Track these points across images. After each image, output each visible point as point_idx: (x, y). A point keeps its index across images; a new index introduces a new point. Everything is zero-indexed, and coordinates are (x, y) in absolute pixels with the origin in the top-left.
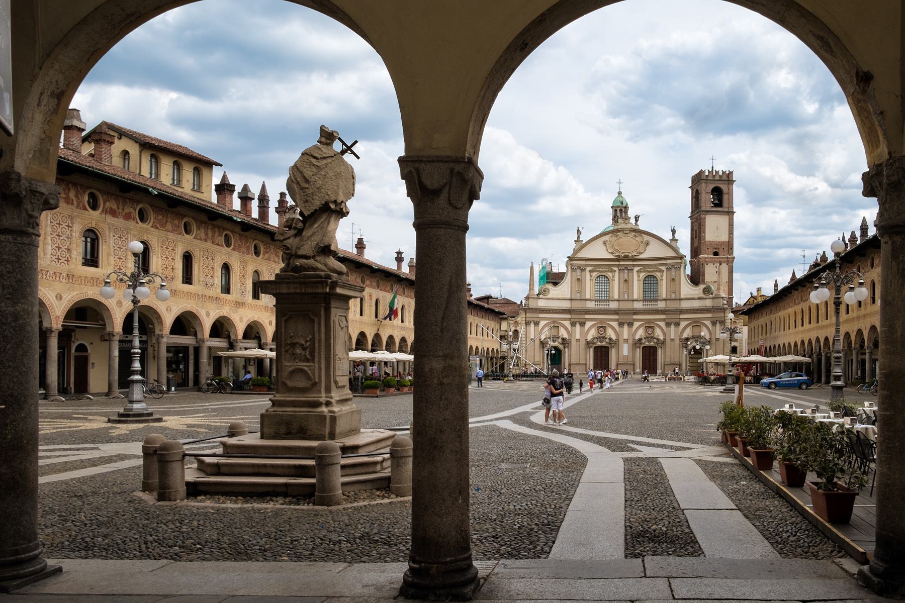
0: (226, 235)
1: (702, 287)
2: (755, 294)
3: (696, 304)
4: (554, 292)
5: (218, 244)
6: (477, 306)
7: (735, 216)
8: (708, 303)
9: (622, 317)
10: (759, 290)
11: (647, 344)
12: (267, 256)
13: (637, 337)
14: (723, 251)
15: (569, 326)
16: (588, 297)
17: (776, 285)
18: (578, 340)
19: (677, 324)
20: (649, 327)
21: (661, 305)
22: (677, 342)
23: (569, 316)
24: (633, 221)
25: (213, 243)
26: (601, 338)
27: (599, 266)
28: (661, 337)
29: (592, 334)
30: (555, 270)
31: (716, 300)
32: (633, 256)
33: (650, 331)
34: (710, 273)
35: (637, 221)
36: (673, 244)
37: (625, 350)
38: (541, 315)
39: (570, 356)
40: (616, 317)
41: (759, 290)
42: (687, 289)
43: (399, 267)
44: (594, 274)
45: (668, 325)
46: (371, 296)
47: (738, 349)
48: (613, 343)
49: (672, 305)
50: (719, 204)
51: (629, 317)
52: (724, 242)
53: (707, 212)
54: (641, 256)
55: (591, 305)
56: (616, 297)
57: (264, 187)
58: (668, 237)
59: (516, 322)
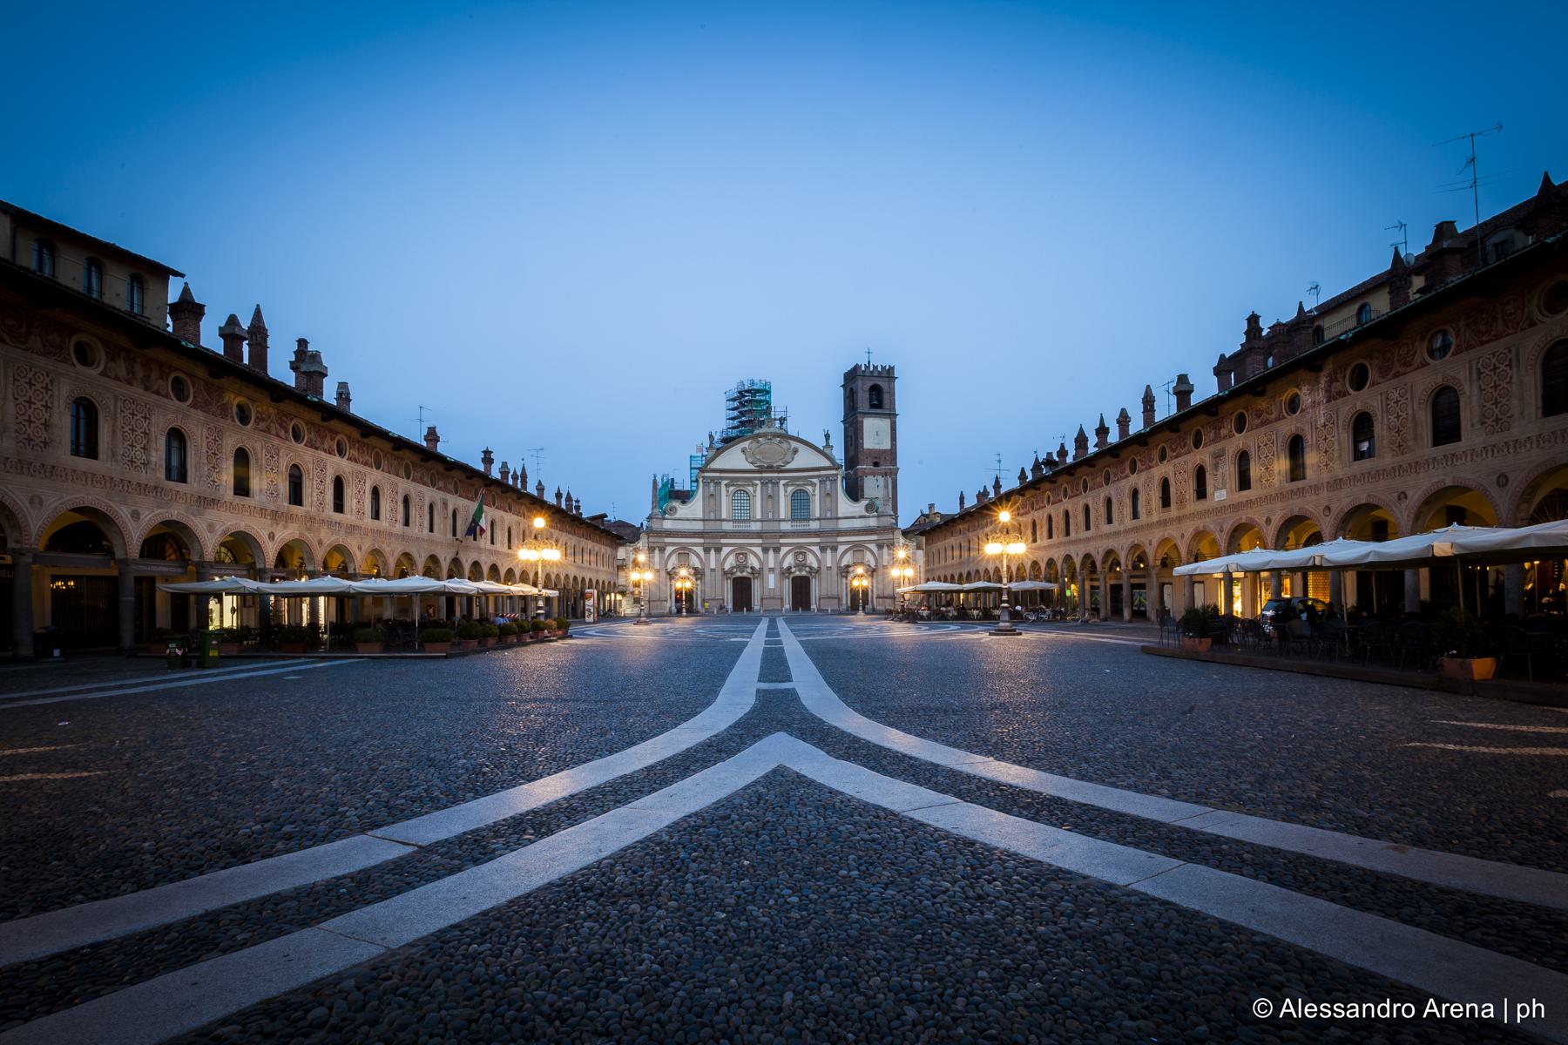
0: (176, 380)
1: (864, 503)
2: (926, 512)
3: (858, 524)
4: (682, 510)
5: (157, 393)
6: (589, 525)
8: (873, 522)
10: (931, 506)
12: (263, 425)
13: (785, 565)
14: (886, 461)
15: (701, 553)
16: (724, 516)
19: (834, 549)
21: (814, 525)
22: (835, 570)
24: (777, 424)
25: (147, 388)
26: (742, 567)
27: (737, 479)
28: (815, 565)
29: (730, 562)
30: (677, 487)
34: (873, 486)
36: (827, 451)
37: (771, 581)
41: (931, 506)
42: (845, 506)
43: (488, 468)
44: (731, 489)
45: (823, 549)
46: (445, 504)
48: (757, 573)
49: (828, 525)
50: (880, 406)
53: (866, 414)
54: (788, 467)
55: (727, 526)
56: (759, 516)
57: (258, 313)
58: (821, 444)
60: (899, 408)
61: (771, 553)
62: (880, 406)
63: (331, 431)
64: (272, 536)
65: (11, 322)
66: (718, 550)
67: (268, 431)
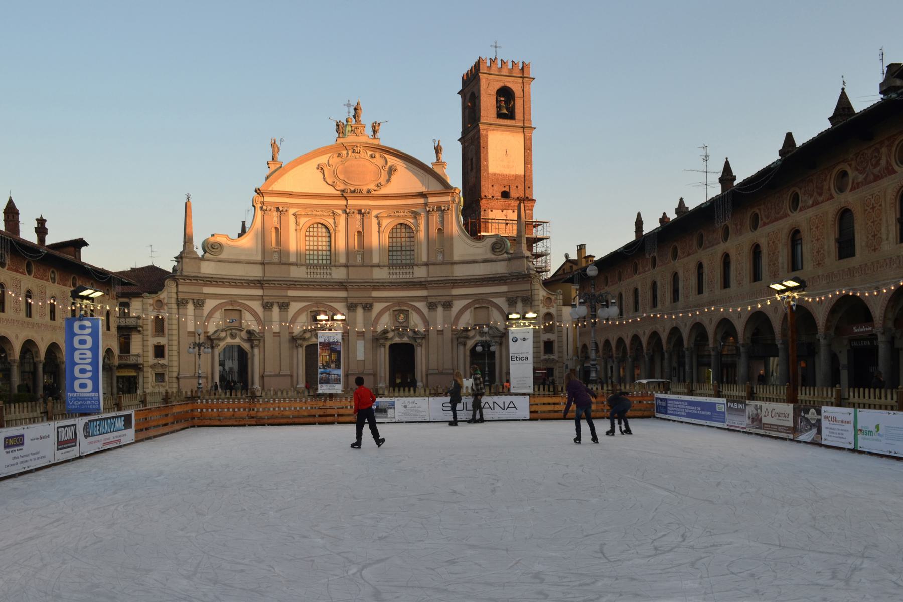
2: (574, 256)
7: (535, 135)
8: (500, 268)
9: (352, 294)
10: (581, 248)
11: (397, 340)
13: (380, 328)
17: (639, 223)
18: (277, 334)
19: (448, 305)
20: (401, 309)
21: (420, 273)
22: (448, 335)
23: (259, 292)
24: (369, 131)
31: (516, 263)
32: (369, 191)
33: (402, 318)
35: (375, 132)
36: (437, 169)
37: (360, 351)
38: (207, 290)
39: (263, 361)
40: (343, 294)
41: (581, 248)
45: (432, 306)
47: (556, 345)
49: (438, 273)
50: (511, 116)
51: (365, 294)
52: (516, 177)
58: (429, 159)
59: (160, 304)
60: (536, 118)
61: (360, 311)
62: (511, 116)
66: (284, 306)
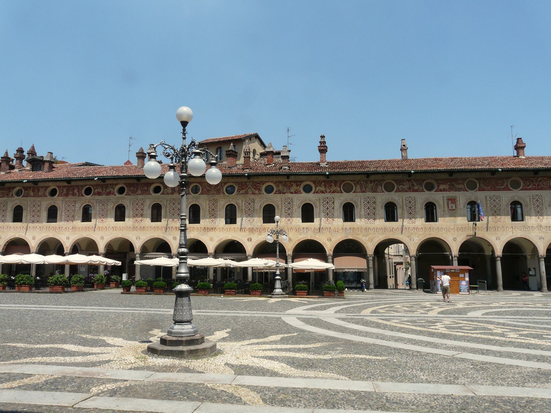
12: (242, 192)
63: (295, 182)
64: (250, 240)
65: (132, 188)
67: (247, 193)
